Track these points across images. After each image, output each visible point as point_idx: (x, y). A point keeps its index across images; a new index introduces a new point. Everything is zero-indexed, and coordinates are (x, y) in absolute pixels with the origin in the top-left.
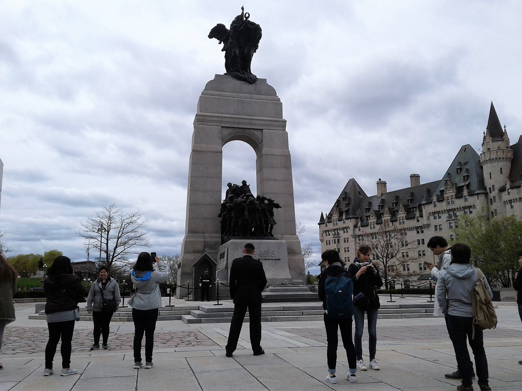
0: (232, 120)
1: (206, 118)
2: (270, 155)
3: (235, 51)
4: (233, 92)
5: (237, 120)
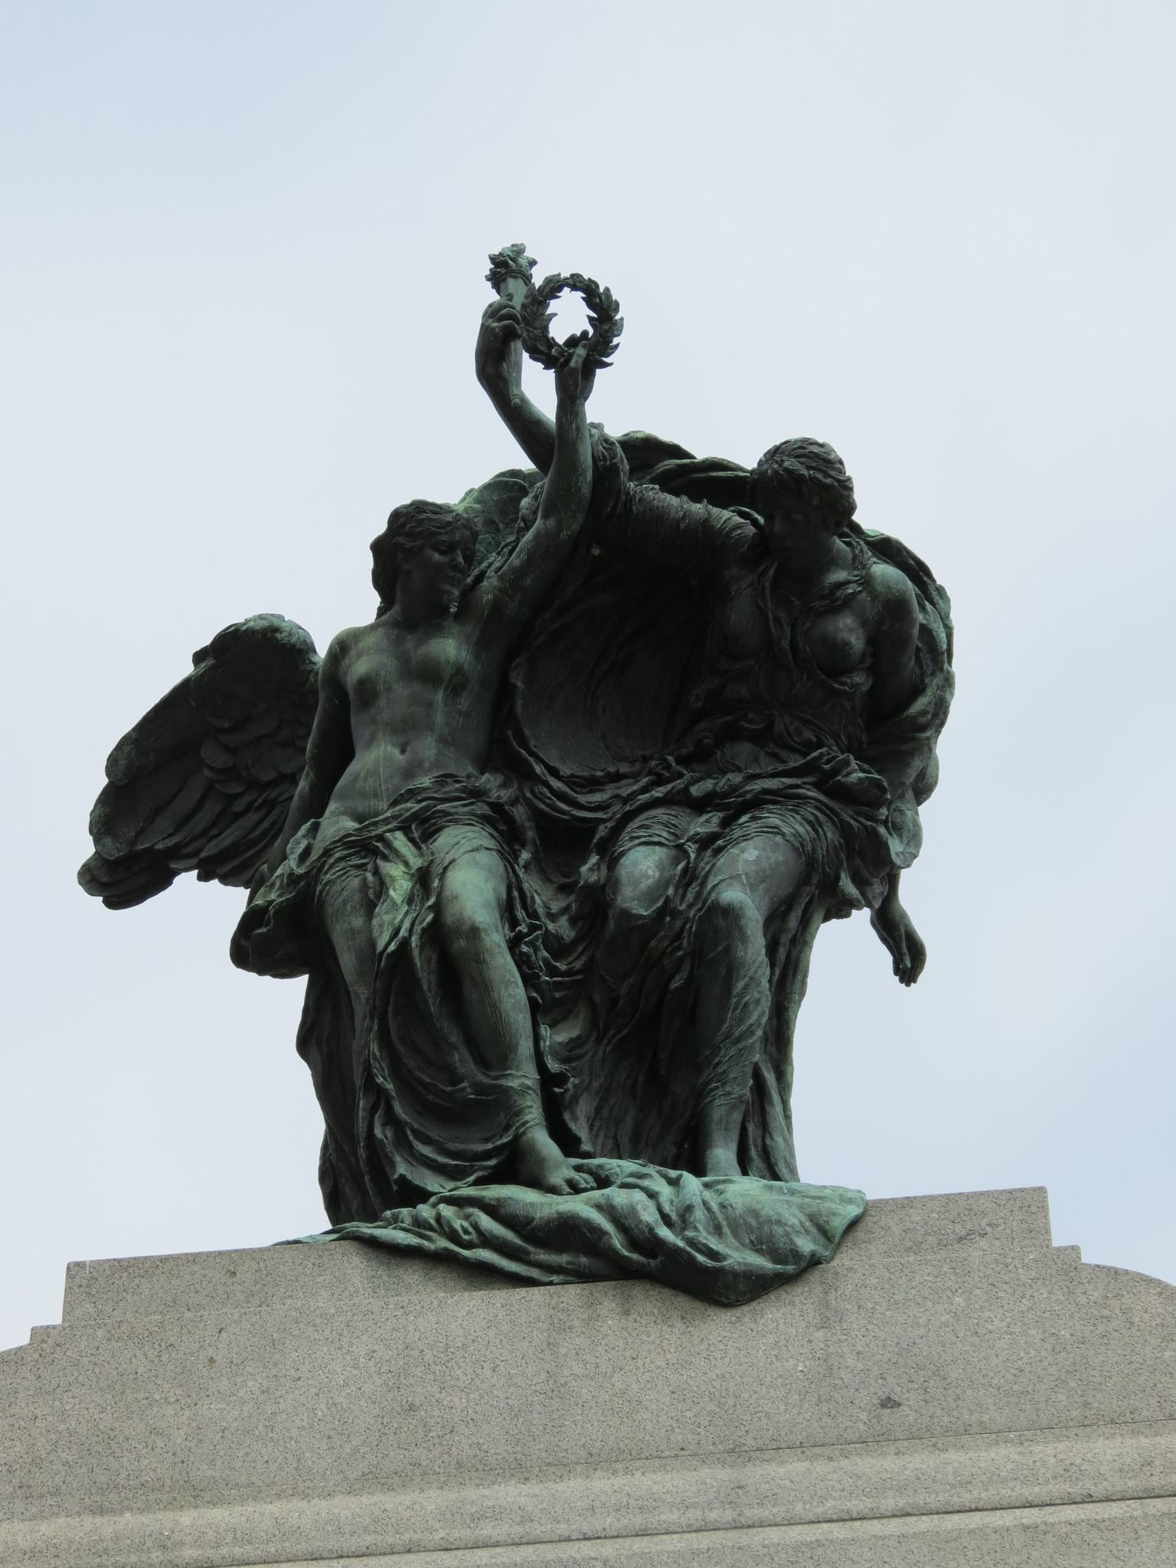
4: (374, 1480)
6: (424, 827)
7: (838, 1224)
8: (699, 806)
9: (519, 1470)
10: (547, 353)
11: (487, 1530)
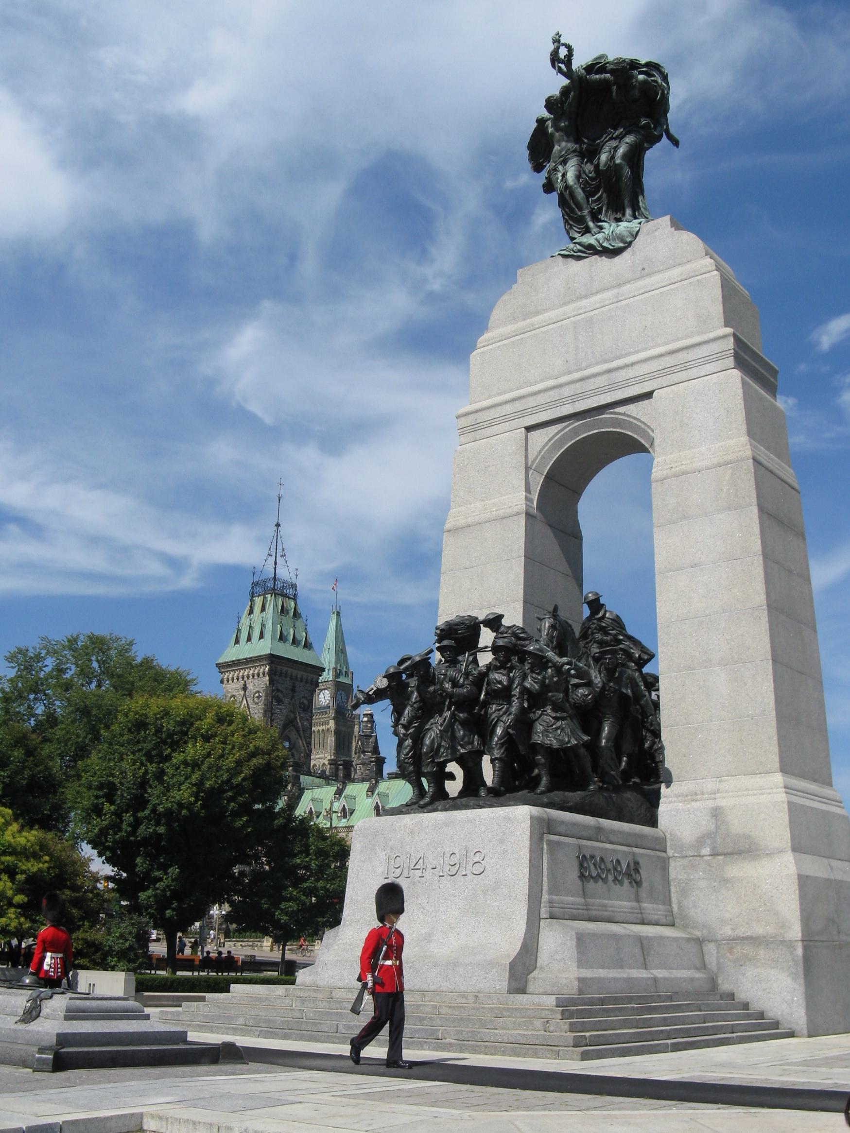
0: (553, 395)
1: (482, 417)
2: (676, 475)
3: (564, 175)
5: (567, 391)
6: (564, 162)
7: (634, 233)
8: (615, 139)
9: (586, 297)
10: (562, 62)
11: (580, 311)
